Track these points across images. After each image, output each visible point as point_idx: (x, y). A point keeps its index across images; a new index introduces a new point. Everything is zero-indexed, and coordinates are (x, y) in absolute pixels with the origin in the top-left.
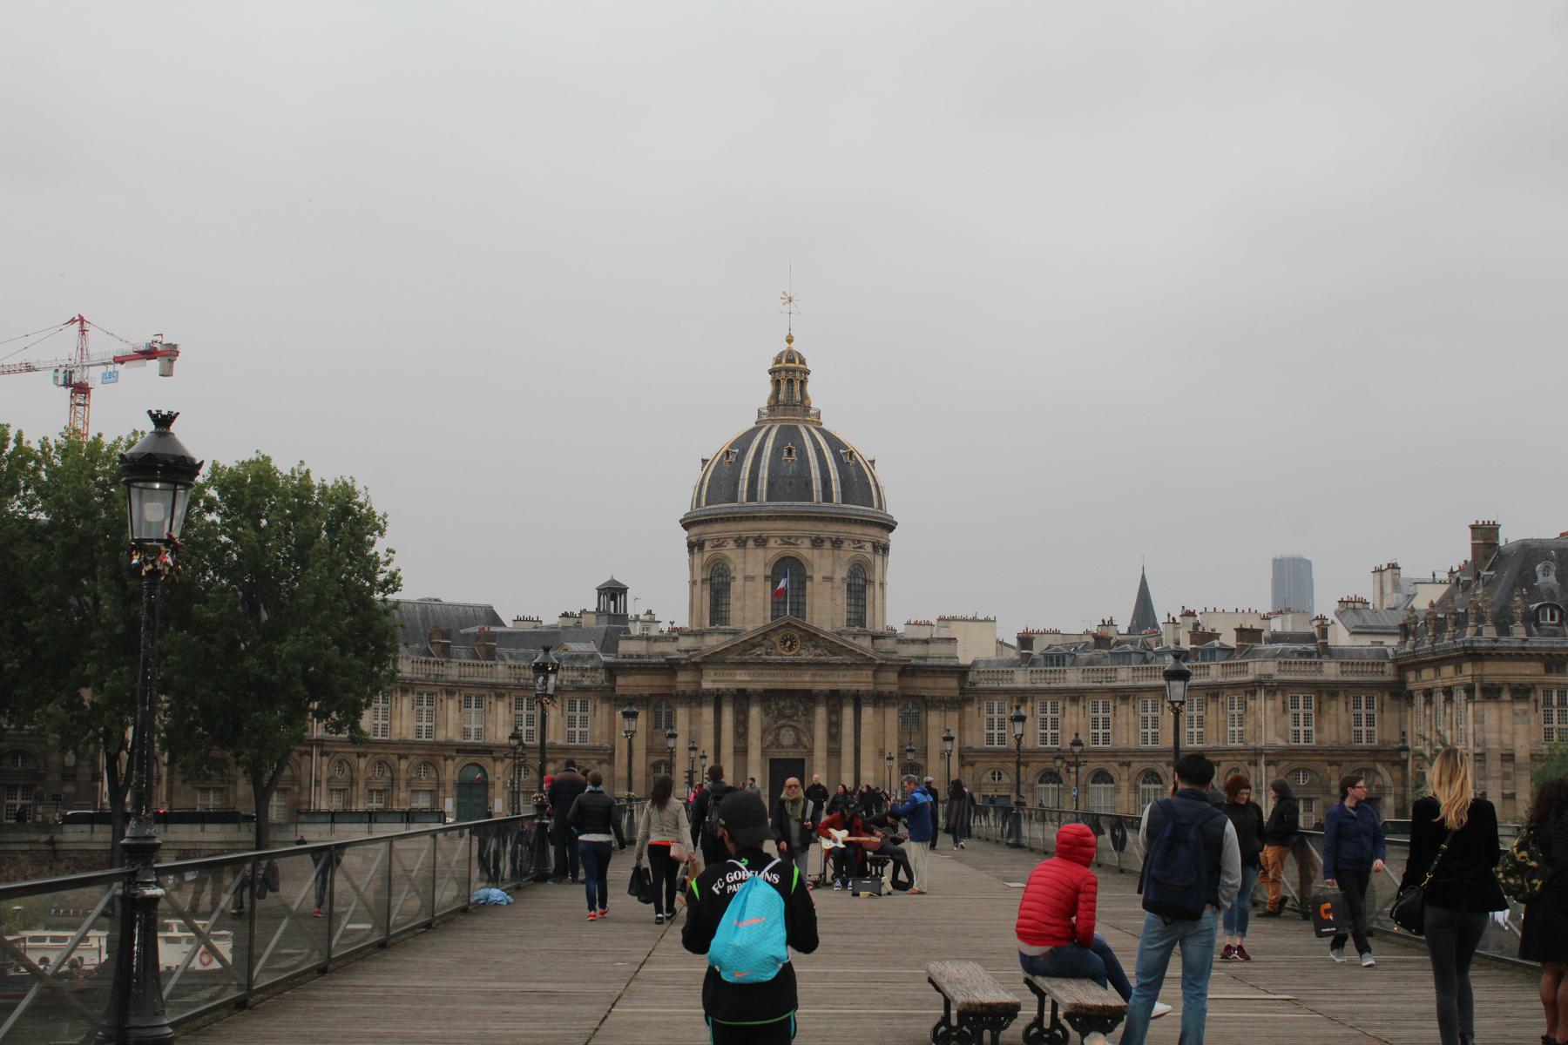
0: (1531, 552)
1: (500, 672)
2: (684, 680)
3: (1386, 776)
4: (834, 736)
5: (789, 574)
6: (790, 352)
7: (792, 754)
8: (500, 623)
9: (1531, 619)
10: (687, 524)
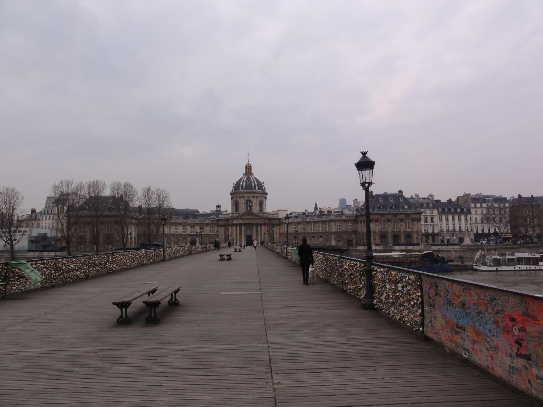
1: (198, 221)
2: (230, 222)
3: (354, 236)
4: (257, 231)
5: (248, 203)
6: (249, 164)
8: (198, 212)
9: (379, 208)
10: (231, 194)
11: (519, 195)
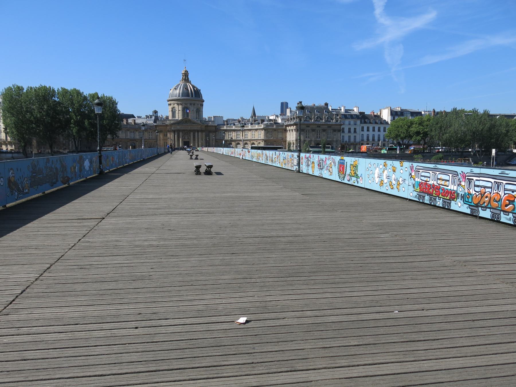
4: (194, 137)
7: (187, 140)
11: (434, 110)
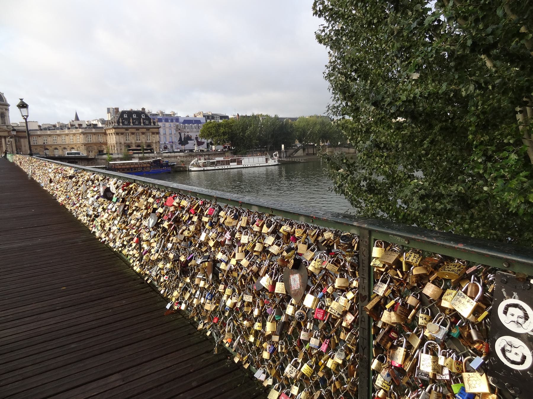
0: (123, 112)
9: (123, 123)
